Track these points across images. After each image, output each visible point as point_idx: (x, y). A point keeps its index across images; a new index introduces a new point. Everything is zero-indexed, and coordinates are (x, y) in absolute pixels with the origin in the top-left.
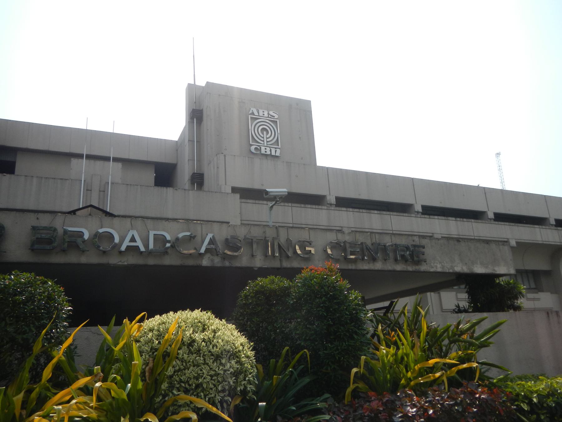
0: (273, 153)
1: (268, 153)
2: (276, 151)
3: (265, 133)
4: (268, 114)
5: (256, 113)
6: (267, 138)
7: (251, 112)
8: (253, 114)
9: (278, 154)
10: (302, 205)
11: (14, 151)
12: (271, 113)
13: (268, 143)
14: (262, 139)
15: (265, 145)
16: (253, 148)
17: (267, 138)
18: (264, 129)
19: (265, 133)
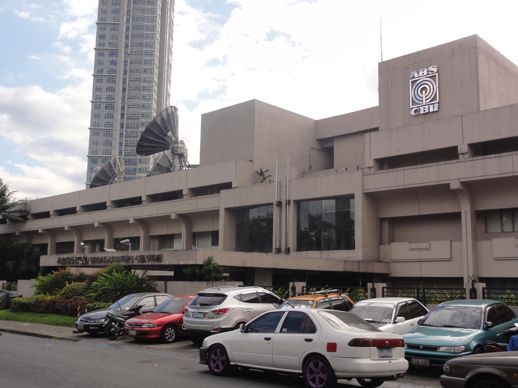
0: (431, 110)
1: (427, 111)
2: (434, 107)
3: (424, 92)
4: (428, 71)
5: (416, 75)
6: (426, 97)
7: (412, 76)
8: (414, 77)
9: (436, 109)
10: (414, 167)
11: (331, 139)
12: (431, 69)
13: (427, 101)
14: (421, 99)
15: (424, 103)
16: (412, 113)
17: (426, 97)
18: (424, 88)
19: (424, 92)
